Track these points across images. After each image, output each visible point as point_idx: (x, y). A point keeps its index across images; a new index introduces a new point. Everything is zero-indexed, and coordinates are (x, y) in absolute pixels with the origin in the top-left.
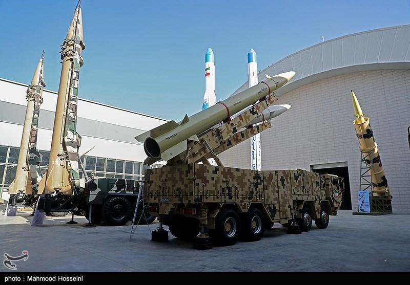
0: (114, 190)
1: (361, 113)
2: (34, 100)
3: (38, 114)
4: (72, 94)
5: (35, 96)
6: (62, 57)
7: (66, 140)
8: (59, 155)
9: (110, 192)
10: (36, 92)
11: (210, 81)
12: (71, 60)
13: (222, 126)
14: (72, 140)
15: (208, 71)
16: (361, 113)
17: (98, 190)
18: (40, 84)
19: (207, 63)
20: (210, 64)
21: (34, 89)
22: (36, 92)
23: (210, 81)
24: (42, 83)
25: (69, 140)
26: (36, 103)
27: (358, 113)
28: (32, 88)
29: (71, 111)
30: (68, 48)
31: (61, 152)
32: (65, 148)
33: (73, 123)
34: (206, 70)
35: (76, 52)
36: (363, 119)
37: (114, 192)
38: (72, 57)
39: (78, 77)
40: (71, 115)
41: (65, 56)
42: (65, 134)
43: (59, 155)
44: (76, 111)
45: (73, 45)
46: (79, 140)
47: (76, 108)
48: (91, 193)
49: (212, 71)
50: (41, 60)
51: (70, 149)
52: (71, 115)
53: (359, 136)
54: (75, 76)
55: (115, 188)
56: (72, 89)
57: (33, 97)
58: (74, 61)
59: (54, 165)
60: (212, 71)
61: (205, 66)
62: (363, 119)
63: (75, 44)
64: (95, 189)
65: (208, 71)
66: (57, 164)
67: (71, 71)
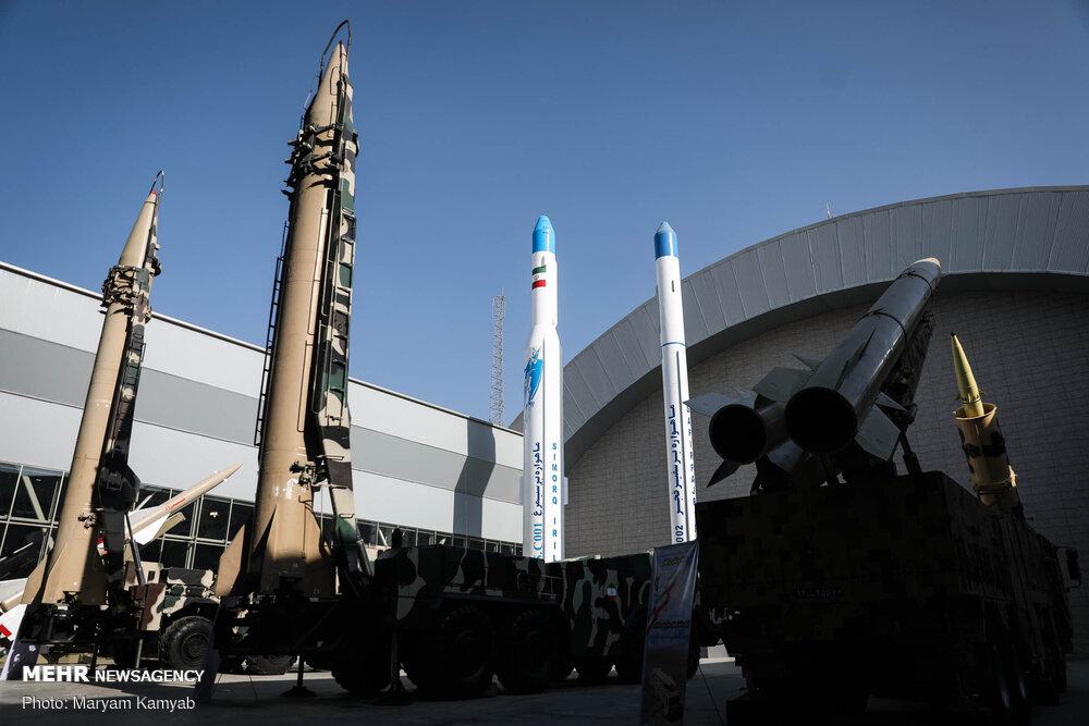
0: (457, 585)
1: (976, 392)
2: (129, 312)
3: (139, 351)
4: (337, 282)
5: (133, 300)
7: (323, 422)
8: (295, 468)
9: (447, 589)
11: (547, 300)
14: (336, 423)
15: (541, 276)
16: (976, 392)
17: (419, 582)
18: (148, 266)
19: (540, 254)
20: (547, 258)
22: (136, 288)
23: (547, 300)
24: (155, 264)
25: (332, 423)
26: (135, 321)
27: (969, 390)
29: (336, 332)
30: (320, 151)
33: (340, 371)
34: (536, 271)
35: (347, 162)
36: (980, 405)
37: (456, 590)
38: (329, 177)
39: (351, 234)
40: (336, 344)
41: (309, 172)
43: (295, 468)
44: (347, 333)
45: (335, 143)
49: (550, 275)
50: (153, 198)
52: (336, 344)
53: (971, 451)
54: (344, 229)
55: (459, 578)
56: (337, 267)
58: (341, 188)
59: (281, 498)
60: (550, 275)
61: (531, 260)
62: (980, 405)
63: (342, 141)
64: (410, 579)
65: (541, 276)
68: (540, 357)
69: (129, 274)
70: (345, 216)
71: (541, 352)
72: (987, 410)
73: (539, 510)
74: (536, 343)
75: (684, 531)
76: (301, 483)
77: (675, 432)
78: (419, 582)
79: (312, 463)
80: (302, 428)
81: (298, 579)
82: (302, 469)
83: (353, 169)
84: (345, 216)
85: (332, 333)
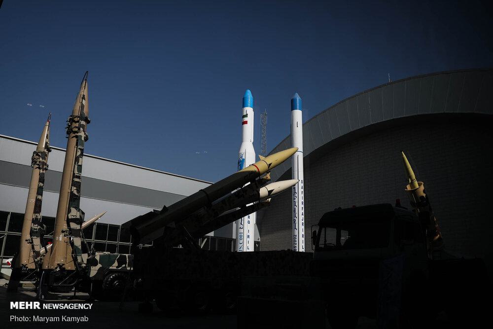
4: (76, 172)
6: (68, 133)
8: (63, 232)
10: (41, 159)
12: (77, 137)
13: (202, 211)
14: (75, 217)
15: (245, 119)
17: (99, 266)
20: (249, 111)
21: (39, 156)
25: (73, 217)
28: (37, 155)
29: (75, 188)
31: (65, 227)
32: (69, 225)
35: (81, 129)
40: (75, 192)
42: (69, 211)
43: (63, 232)
44: (80, 188)
46: (82, 216)
47: (80, 185)
48: (93, 268)
51: (73, 226)
55: (116, 264)
57: (38, 165)
61: (242, 111)
64: (96, 264)
65: (245, 119)
66: (61, 239)
67: (76, 149)
68: (244, 158)
69: (39, 154)
70: (79, 149)
71: (244, 154)
72: (420, 185)
73: (241, 226)
74: (242, 151)
75: (297, 237)
76: (65, 236)
77: (295, 193)
78: (99, 266)
79: (68, 230)
80: (66, 220)
81: (63, 265)
82: (65, 232)
83: (84, 131)
84: (79, 149)
85: (74, 188)
